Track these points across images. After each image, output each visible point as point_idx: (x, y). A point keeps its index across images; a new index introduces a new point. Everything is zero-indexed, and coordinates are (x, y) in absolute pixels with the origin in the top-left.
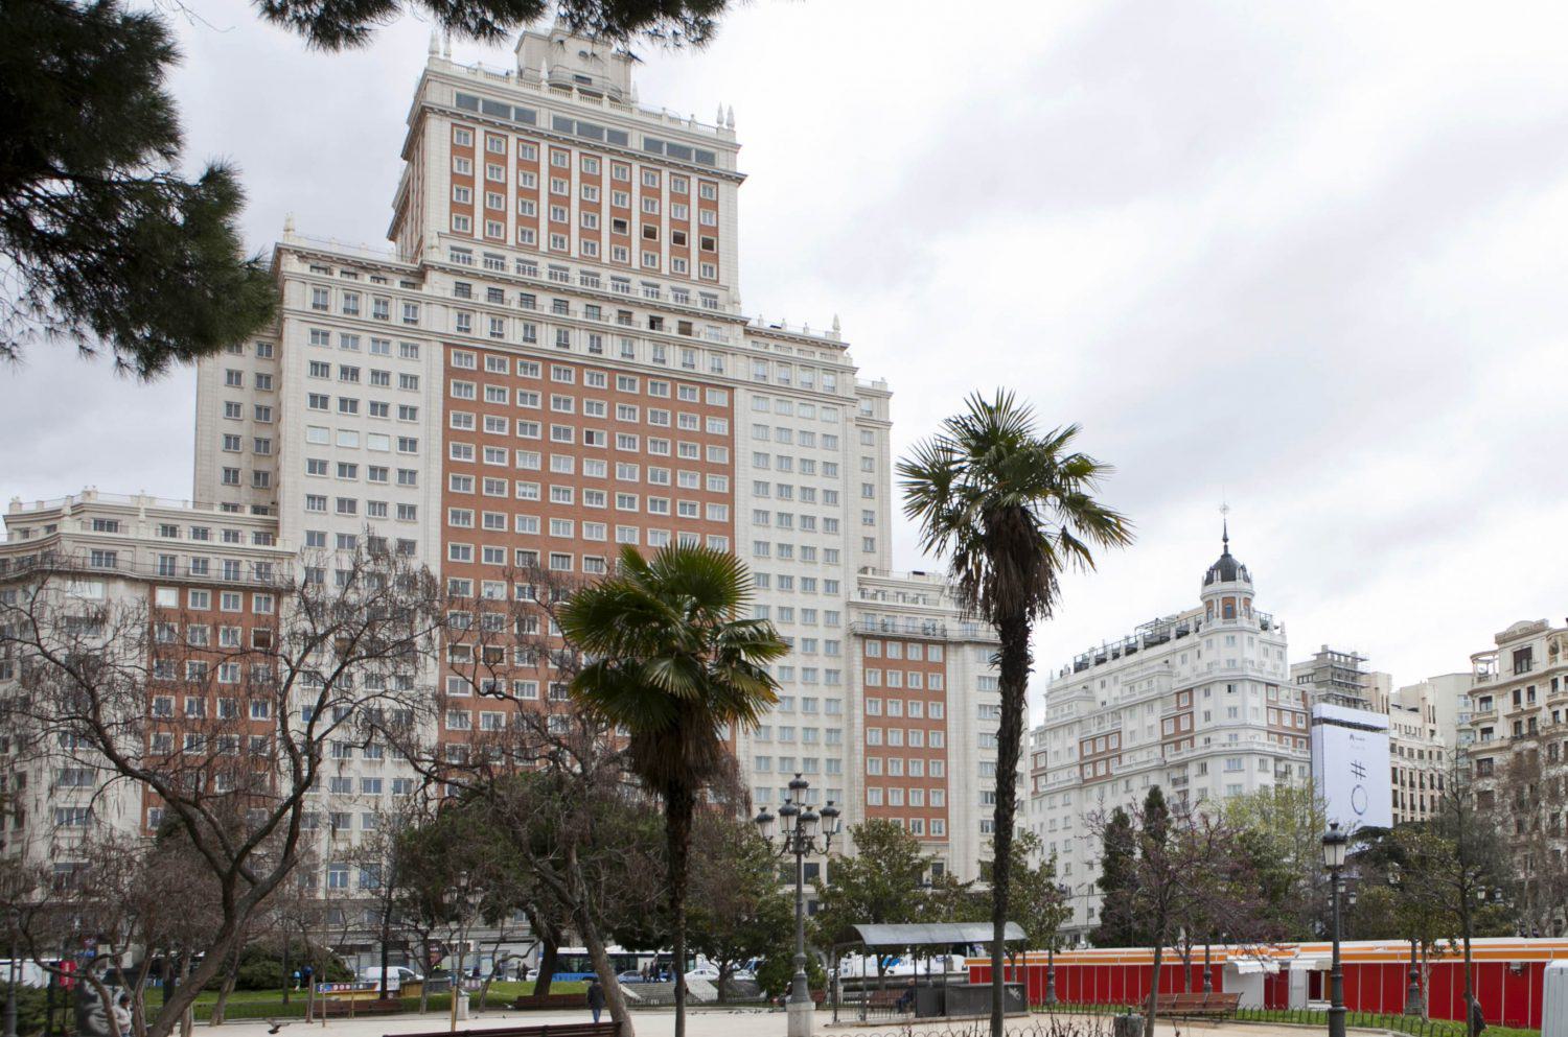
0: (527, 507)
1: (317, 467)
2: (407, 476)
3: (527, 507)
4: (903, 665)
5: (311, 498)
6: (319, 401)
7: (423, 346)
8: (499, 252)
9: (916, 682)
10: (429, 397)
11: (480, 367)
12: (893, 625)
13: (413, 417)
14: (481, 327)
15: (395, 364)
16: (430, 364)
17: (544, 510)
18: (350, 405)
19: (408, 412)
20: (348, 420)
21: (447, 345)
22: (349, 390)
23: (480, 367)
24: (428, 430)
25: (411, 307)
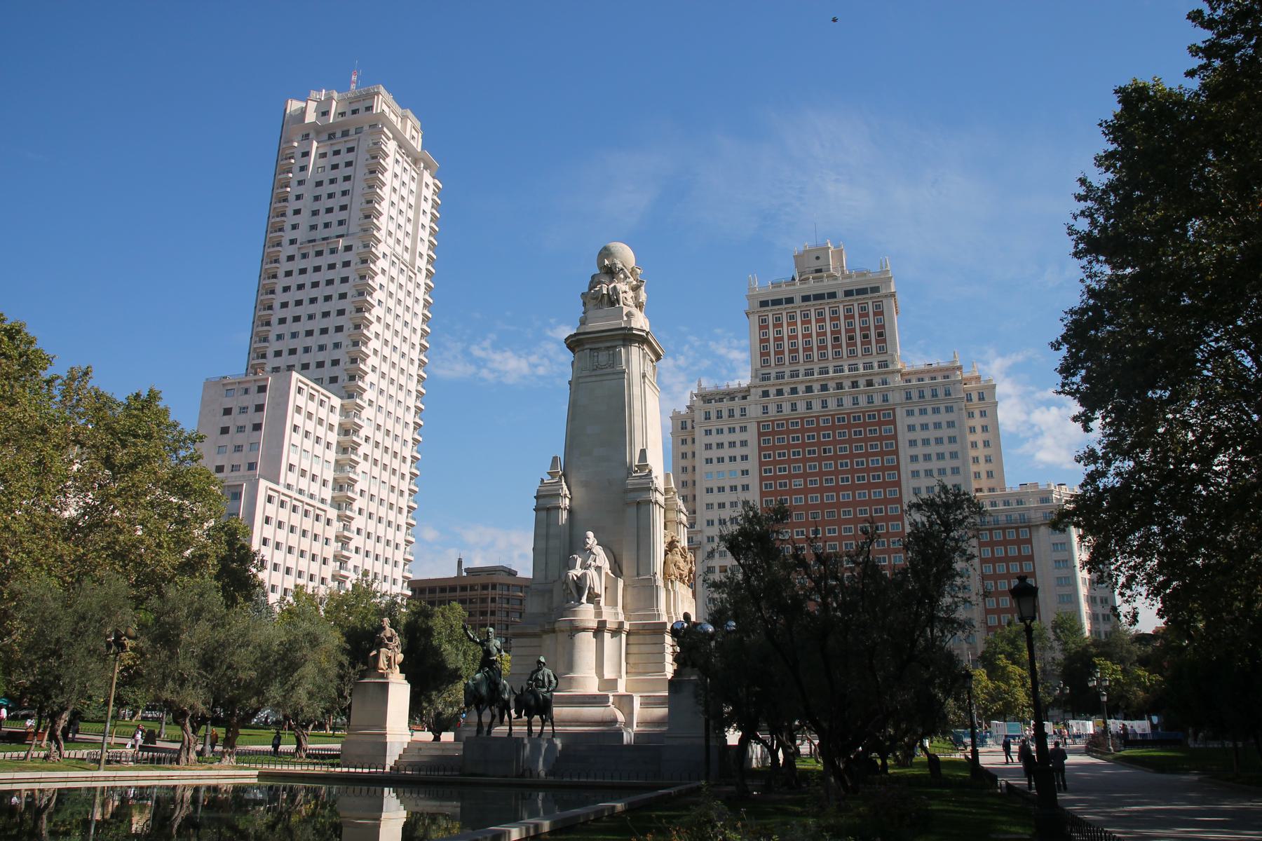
0: (798, 492)
1: (709, 490)
2: (746, 488)
3: (798, 492)
4: (1005, 543)
5: (707, 505)
6: (709, 461)
7: (748, 425)
8: (782, 370)
9: (1013, 551)
10: (752, 451)
11: (773, 428)
12: (998, 521)
13: (747, 459)
14: (772, 409)
15: (738, 437)
16: (751, 435)
17: (805, 491)
18: (721, 460)
19: (745, 458)
20: (721, 467)
21: (759, 423)
22: (721, 453)
23: (773, 428)
24: (752, 465)
25: (743, 410)
